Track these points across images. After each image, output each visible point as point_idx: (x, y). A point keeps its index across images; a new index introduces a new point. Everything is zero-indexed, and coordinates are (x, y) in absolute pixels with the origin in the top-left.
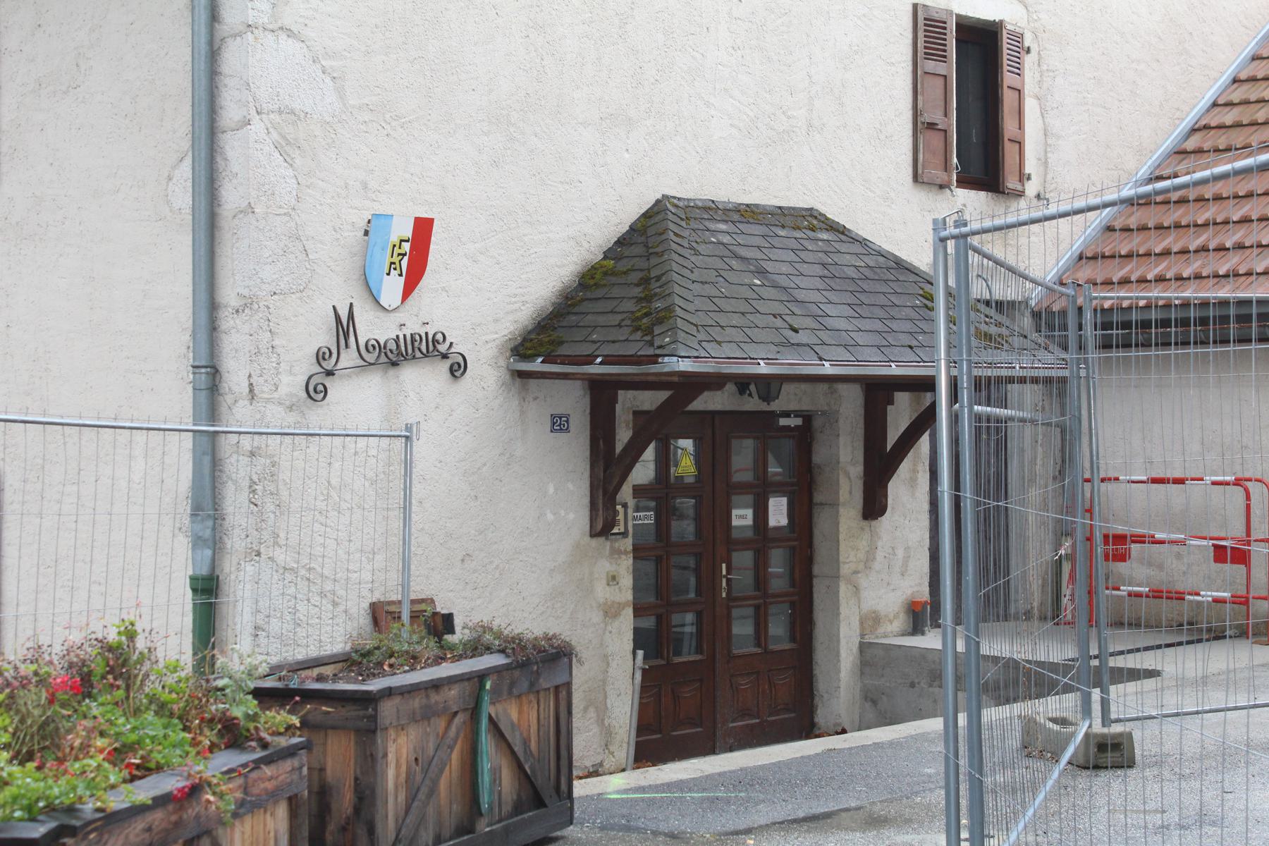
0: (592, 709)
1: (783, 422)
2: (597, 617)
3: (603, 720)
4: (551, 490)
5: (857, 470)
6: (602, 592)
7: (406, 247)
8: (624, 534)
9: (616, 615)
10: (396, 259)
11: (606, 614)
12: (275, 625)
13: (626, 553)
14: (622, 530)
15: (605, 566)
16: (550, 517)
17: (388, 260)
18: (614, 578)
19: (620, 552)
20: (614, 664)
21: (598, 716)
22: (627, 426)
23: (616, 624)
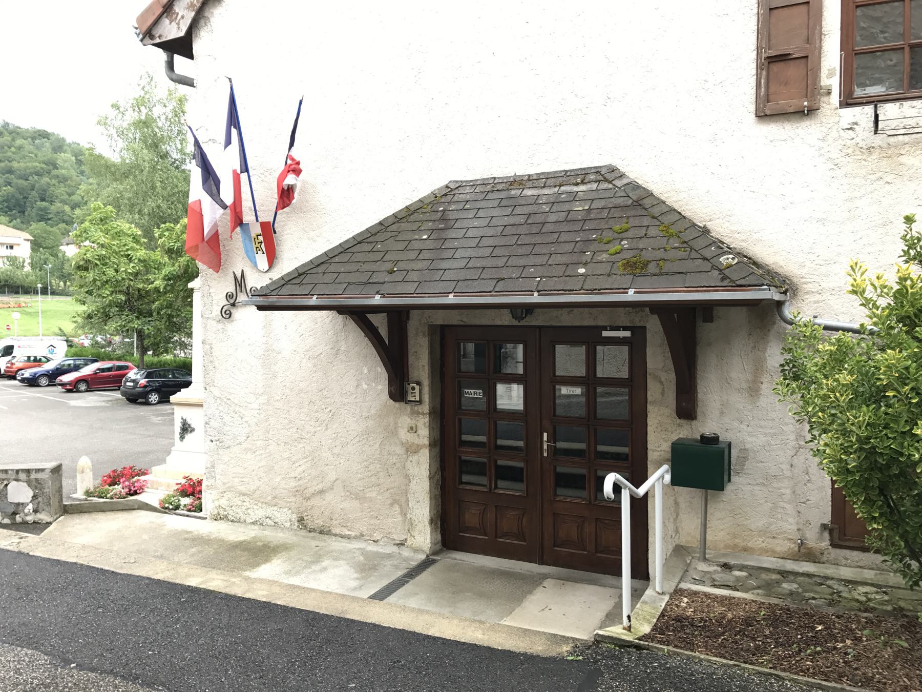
1: (605, 334)
2: (400, 450)
3: (405, 514)
4: (366, 371)
5: (670, 378)
6: (404, 434)
7: (261, 238)
8: (420, 402)
10: (258, 245)
11: (407, 450)
12: (212, 423)
13: (423, 414)
14: (418, 399)
15: (406, 421)
16: (365, 386)
17: (255, 247)
18: (412, 428)
19: (418, 413)
21: (402, 511)
22: (424, 334)
23: (416, 457)
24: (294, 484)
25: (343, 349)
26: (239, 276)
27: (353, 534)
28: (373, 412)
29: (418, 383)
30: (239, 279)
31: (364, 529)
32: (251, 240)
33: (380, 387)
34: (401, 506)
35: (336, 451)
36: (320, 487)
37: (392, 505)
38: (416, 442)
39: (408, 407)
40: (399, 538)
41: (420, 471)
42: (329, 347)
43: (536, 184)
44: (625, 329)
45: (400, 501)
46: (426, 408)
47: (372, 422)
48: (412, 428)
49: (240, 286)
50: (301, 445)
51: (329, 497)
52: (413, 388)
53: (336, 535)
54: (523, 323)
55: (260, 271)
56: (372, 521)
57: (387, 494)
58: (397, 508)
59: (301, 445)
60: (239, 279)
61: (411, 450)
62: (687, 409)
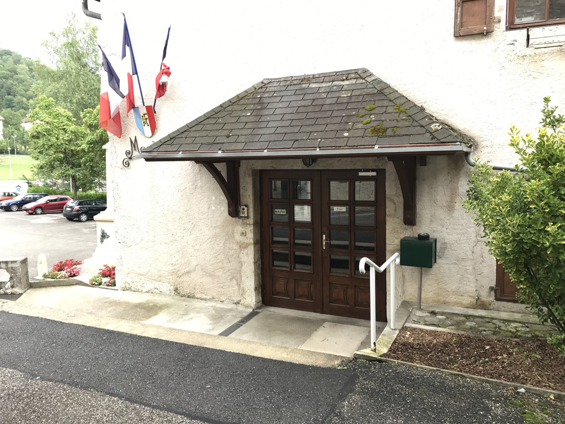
0: (234, 280)
1: (361, 174)
2: (236, 247)
3: (240, 285)
4: (214, 199)
5: (400, 200)
6: (238, 237)
7: (146, 116)
8: (248, 217)
9: (246, 248)
10: (145, 121)
11: (240, 246)
13: (250, 224)
14: (246, 216)
15: (239, 229)
16: (213, 208)
17: (143, 122)
18: (243, 233)
20: (245, 266)
21: (237, 283)
22: (249, 175)
23: (246, 251)
24: (172, 268)
25: (199, 185)
26: (133, 140)
27: (208, 297)
28: (219, 224)
29: (246, 206)
30: (134, 142)
31: (215, 295)
32: (140, 118)
33: (223, 209)
34: (237, 280)
35: (197, 247)
36: (187, 269)
37: (231, 279)
38: (246, 242)
39: (241, 221)
40: (236, 299)
41: (248, 258)
42: (191, 184)
43: (318, 80)
44: (373, 170)
45: (237, 277)
46: (251, 221)
47: (219, 230)
48: (243, 233)
49: (135, 146)
50: (175, 244)
51: (193, 275)
52: (243, 209)
53: (197, 298)
54: (310, 168)
55: (147, 137)
56: (220, 290)
57: (229, 273)
58: (234, 281)
59: (175, 244)
60: (134, 142)
61: (243, 246)
62: (410, 218)
